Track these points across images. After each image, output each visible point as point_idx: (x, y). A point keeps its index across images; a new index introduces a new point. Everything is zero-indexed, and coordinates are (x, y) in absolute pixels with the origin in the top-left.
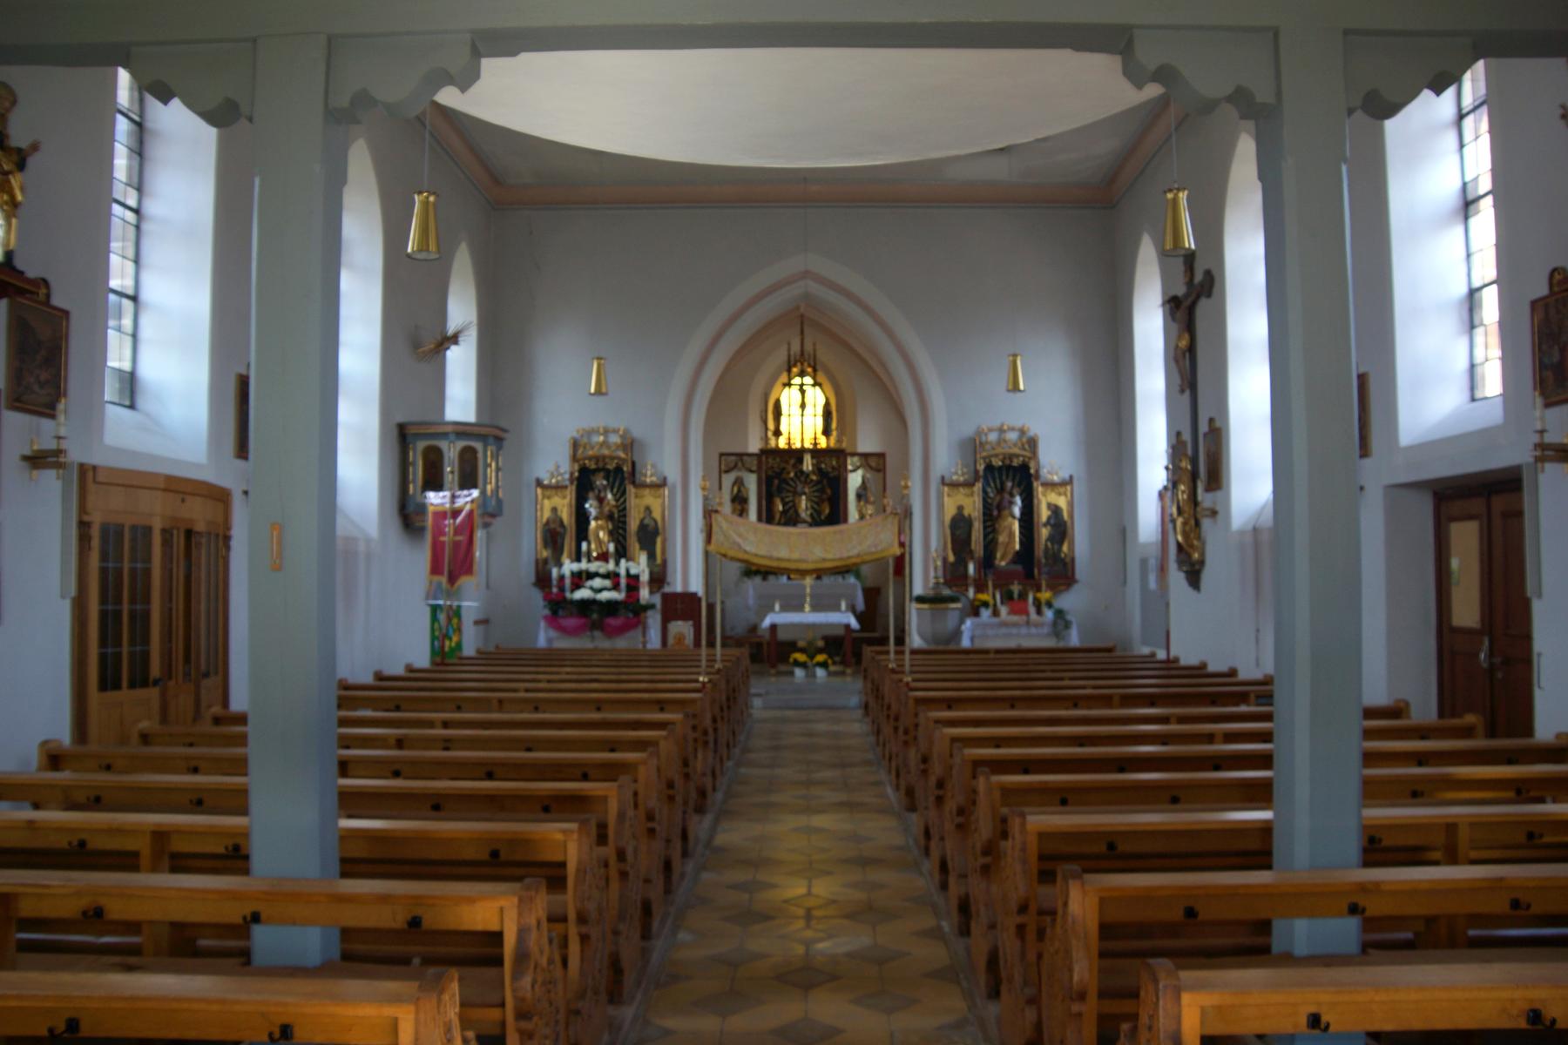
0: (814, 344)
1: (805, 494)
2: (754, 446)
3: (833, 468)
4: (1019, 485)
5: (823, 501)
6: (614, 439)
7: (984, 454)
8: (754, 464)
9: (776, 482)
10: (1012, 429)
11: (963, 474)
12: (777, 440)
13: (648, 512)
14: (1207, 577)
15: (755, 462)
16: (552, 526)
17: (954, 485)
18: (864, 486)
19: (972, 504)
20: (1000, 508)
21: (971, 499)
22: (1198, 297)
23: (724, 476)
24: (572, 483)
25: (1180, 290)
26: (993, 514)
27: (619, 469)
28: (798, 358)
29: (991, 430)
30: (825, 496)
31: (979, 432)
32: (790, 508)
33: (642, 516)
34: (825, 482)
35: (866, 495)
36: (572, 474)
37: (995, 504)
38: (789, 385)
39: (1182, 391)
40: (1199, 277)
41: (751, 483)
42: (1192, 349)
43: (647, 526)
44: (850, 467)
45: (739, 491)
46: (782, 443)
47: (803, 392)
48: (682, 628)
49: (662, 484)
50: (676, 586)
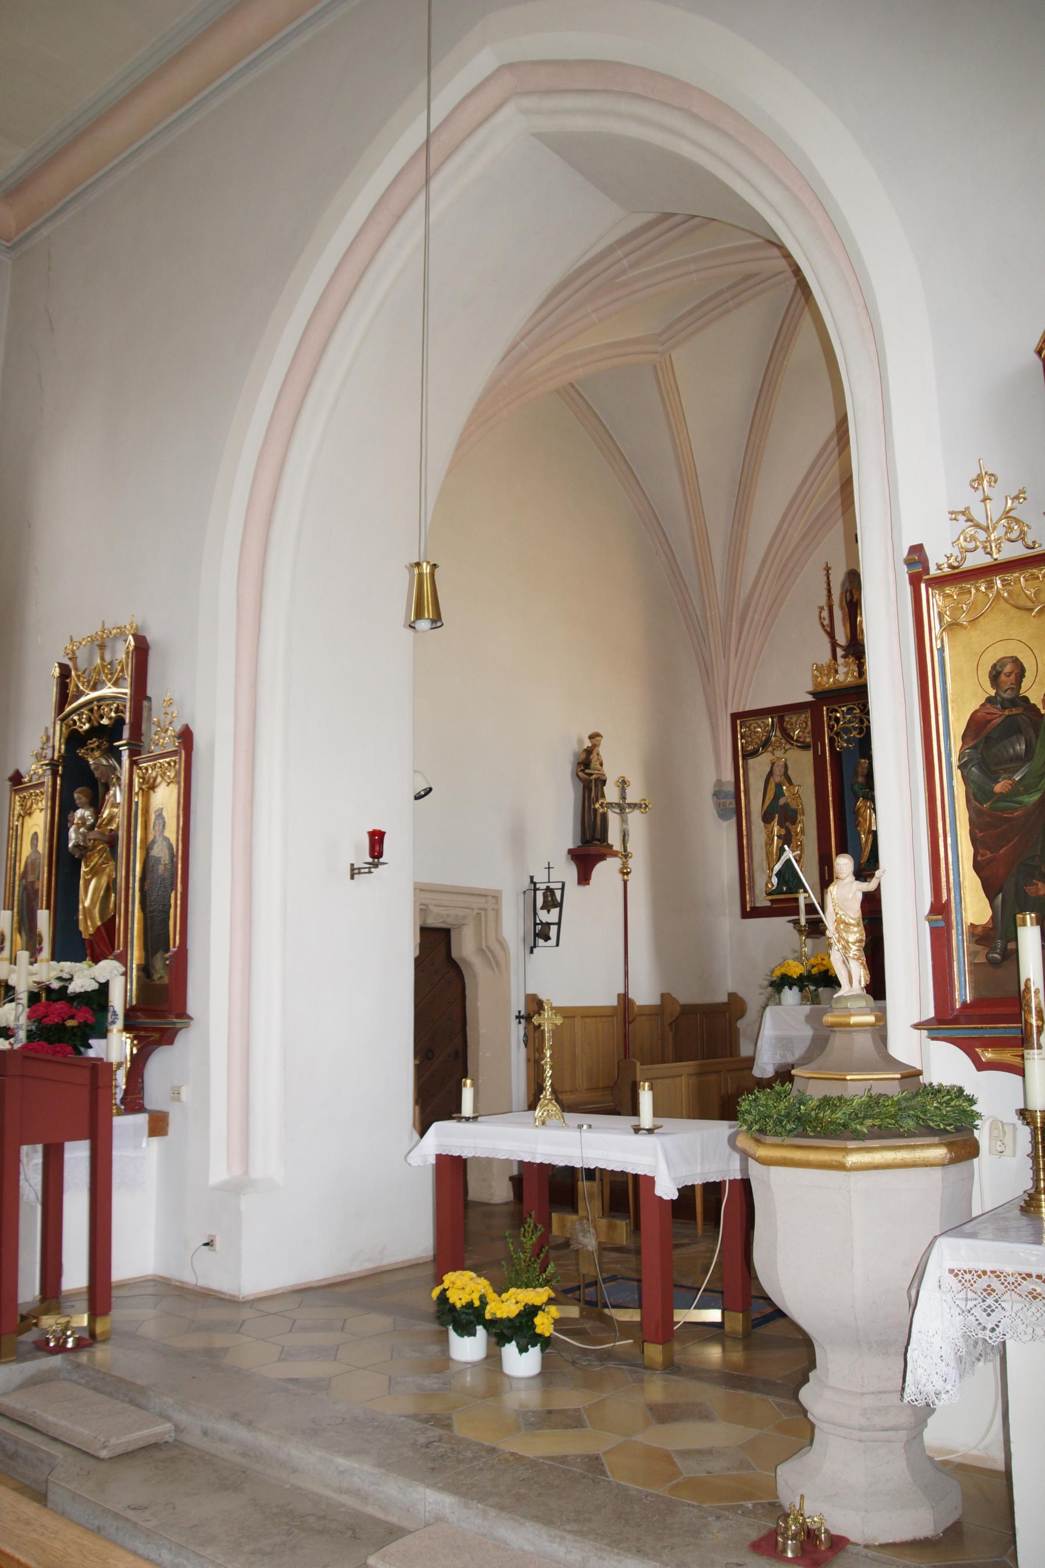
17: (958, 577)
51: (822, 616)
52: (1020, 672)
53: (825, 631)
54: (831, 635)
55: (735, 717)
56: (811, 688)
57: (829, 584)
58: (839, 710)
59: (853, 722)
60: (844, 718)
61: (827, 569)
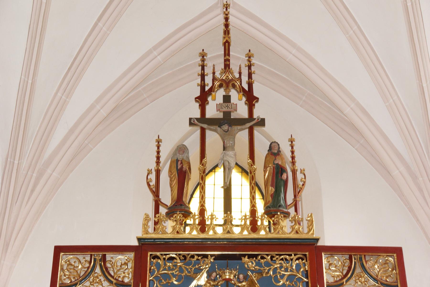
15: (130, 265)
51: (149, 177)
53: (151, 190)
54: (156, 193)
56: (140, 235)
57: (158, 152)
58: (162, 258)
59: (173, 270)
60: (165, 265)
61: (159, 141)
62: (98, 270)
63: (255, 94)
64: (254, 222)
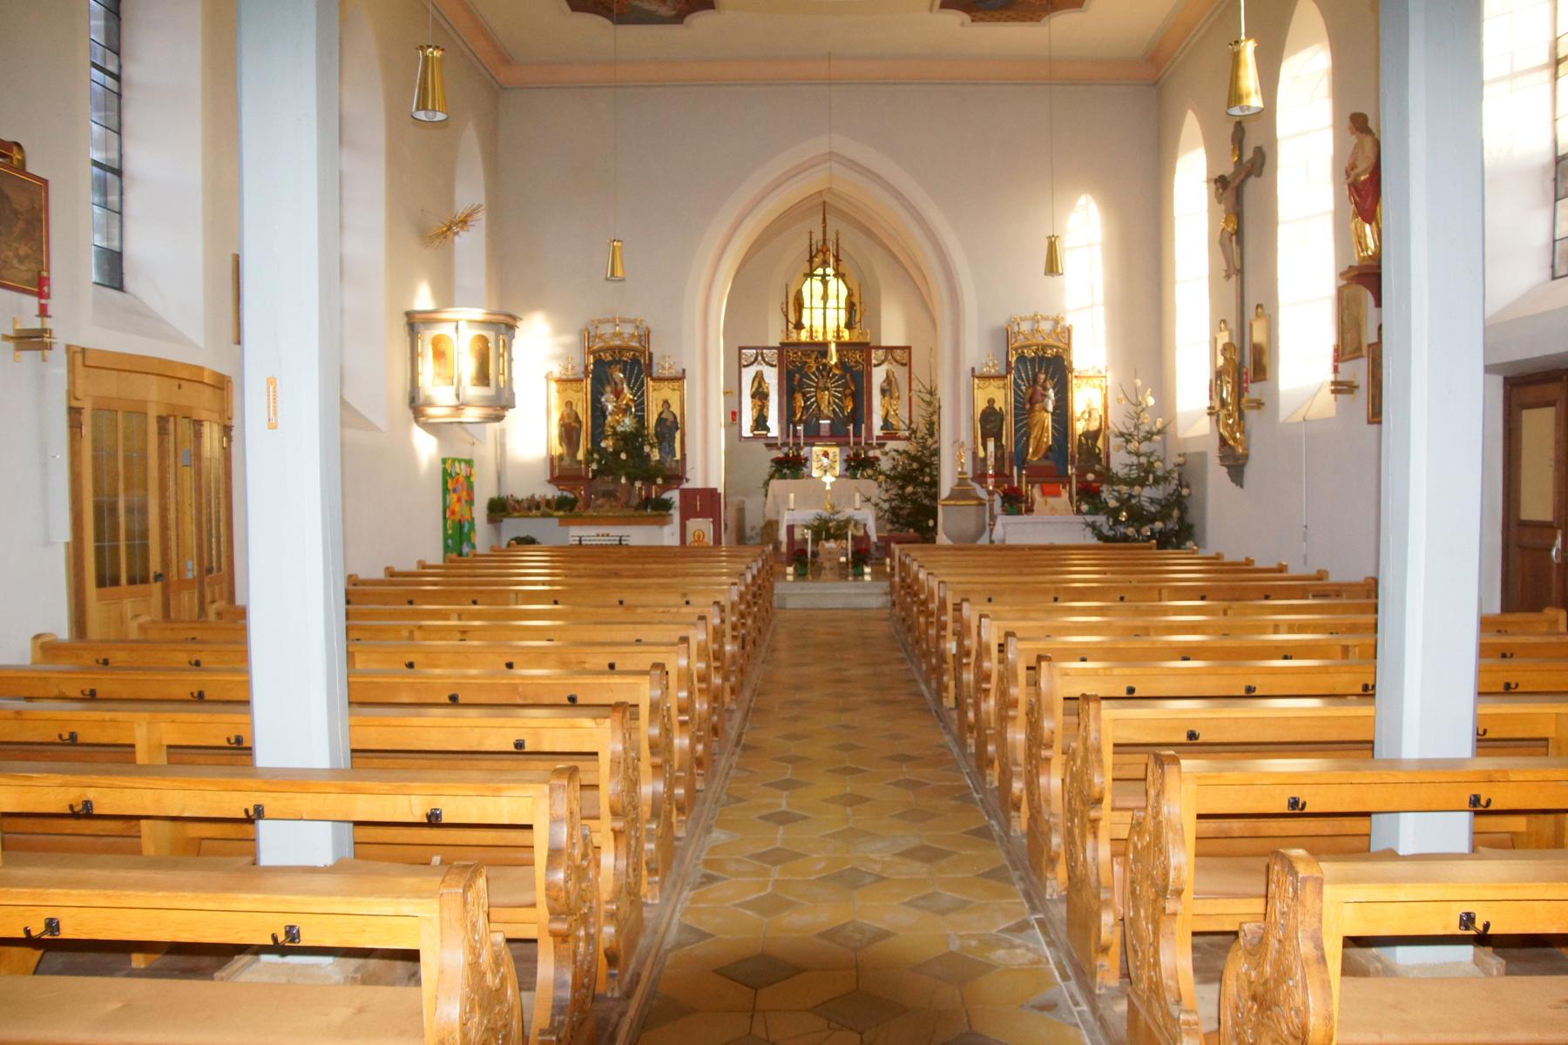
0: (837, 233)
1: (828, 389)
2: (775, 339)
3: (856, 362)
4: (1052, 379)
5: (846, 396)
6: (628, 330)
7: (1016, 345)
8: (771, 355)
9: (797, 375)
10: (1046, 319)
11: (994, 365)
12: (799, 334)
13: (666, 405)
14: (1250, 472)
15: (776, 356)
16: (567, 421)
17: (983, 377)
18: (889, 380)
19: (1001, 397)
20: (1032, 401)
21: (1003, 391)
22: (1248, 175)
23: (744, 370)
24: (587, 377)
25: (1228, 169)
26: (1026, 406)
27: (635, 361)
28: (820, 248)
29: (1023, 320)
30: (848, 391)
31: (1013, 321)
32: (812, 403)
33: (660, 410)
34: (848, 375)
35: (890, 391)
36: (586, 367)
37: (1028, 397)
38: (811, 275)
39: (1228, 277)
40: (1248, 155)
41: (771, 377)
42: (1239, 233)
43: (666, 420)
44: (874, 362)
45: (760, 385)
46: (804, 336)
47: (825, 283)
48: (701, 527)
49: (680, 378)
50: (695, 480)
52: (994, 401)
55: (741, 349)
62: (760, 358)
63: (841, 257)
64: (838, 334)
